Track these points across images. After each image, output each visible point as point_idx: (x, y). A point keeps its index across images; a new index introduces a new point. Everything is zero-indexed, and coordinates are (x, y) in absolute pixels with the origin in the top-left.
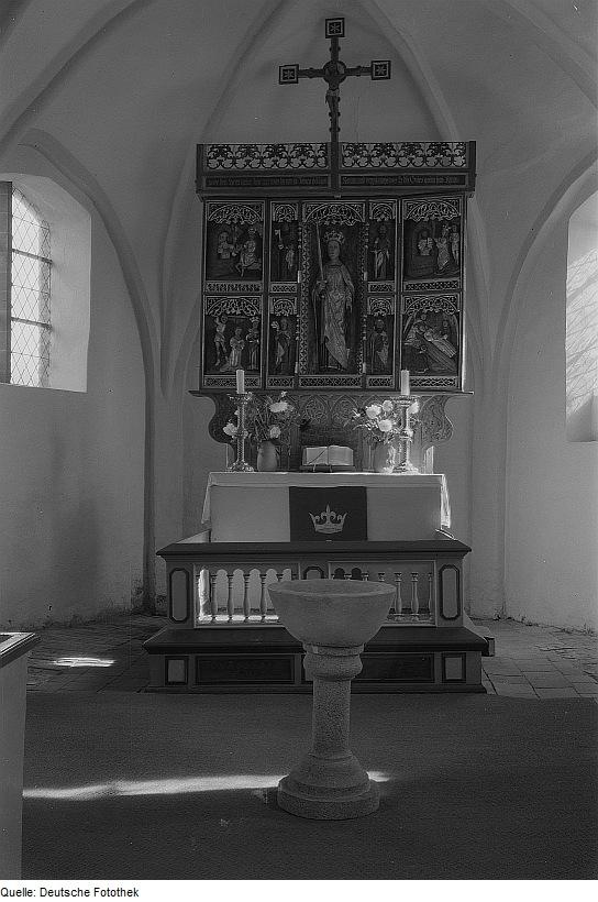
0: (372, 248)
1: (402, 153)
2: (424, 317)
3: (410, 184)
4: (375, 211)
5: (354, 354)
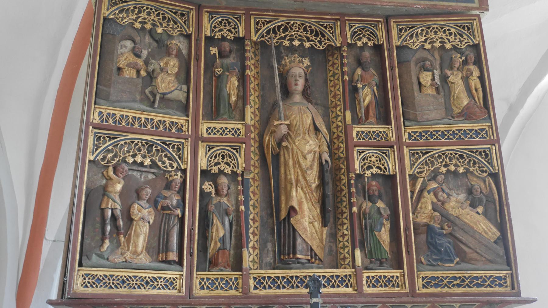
2: (441, 178)
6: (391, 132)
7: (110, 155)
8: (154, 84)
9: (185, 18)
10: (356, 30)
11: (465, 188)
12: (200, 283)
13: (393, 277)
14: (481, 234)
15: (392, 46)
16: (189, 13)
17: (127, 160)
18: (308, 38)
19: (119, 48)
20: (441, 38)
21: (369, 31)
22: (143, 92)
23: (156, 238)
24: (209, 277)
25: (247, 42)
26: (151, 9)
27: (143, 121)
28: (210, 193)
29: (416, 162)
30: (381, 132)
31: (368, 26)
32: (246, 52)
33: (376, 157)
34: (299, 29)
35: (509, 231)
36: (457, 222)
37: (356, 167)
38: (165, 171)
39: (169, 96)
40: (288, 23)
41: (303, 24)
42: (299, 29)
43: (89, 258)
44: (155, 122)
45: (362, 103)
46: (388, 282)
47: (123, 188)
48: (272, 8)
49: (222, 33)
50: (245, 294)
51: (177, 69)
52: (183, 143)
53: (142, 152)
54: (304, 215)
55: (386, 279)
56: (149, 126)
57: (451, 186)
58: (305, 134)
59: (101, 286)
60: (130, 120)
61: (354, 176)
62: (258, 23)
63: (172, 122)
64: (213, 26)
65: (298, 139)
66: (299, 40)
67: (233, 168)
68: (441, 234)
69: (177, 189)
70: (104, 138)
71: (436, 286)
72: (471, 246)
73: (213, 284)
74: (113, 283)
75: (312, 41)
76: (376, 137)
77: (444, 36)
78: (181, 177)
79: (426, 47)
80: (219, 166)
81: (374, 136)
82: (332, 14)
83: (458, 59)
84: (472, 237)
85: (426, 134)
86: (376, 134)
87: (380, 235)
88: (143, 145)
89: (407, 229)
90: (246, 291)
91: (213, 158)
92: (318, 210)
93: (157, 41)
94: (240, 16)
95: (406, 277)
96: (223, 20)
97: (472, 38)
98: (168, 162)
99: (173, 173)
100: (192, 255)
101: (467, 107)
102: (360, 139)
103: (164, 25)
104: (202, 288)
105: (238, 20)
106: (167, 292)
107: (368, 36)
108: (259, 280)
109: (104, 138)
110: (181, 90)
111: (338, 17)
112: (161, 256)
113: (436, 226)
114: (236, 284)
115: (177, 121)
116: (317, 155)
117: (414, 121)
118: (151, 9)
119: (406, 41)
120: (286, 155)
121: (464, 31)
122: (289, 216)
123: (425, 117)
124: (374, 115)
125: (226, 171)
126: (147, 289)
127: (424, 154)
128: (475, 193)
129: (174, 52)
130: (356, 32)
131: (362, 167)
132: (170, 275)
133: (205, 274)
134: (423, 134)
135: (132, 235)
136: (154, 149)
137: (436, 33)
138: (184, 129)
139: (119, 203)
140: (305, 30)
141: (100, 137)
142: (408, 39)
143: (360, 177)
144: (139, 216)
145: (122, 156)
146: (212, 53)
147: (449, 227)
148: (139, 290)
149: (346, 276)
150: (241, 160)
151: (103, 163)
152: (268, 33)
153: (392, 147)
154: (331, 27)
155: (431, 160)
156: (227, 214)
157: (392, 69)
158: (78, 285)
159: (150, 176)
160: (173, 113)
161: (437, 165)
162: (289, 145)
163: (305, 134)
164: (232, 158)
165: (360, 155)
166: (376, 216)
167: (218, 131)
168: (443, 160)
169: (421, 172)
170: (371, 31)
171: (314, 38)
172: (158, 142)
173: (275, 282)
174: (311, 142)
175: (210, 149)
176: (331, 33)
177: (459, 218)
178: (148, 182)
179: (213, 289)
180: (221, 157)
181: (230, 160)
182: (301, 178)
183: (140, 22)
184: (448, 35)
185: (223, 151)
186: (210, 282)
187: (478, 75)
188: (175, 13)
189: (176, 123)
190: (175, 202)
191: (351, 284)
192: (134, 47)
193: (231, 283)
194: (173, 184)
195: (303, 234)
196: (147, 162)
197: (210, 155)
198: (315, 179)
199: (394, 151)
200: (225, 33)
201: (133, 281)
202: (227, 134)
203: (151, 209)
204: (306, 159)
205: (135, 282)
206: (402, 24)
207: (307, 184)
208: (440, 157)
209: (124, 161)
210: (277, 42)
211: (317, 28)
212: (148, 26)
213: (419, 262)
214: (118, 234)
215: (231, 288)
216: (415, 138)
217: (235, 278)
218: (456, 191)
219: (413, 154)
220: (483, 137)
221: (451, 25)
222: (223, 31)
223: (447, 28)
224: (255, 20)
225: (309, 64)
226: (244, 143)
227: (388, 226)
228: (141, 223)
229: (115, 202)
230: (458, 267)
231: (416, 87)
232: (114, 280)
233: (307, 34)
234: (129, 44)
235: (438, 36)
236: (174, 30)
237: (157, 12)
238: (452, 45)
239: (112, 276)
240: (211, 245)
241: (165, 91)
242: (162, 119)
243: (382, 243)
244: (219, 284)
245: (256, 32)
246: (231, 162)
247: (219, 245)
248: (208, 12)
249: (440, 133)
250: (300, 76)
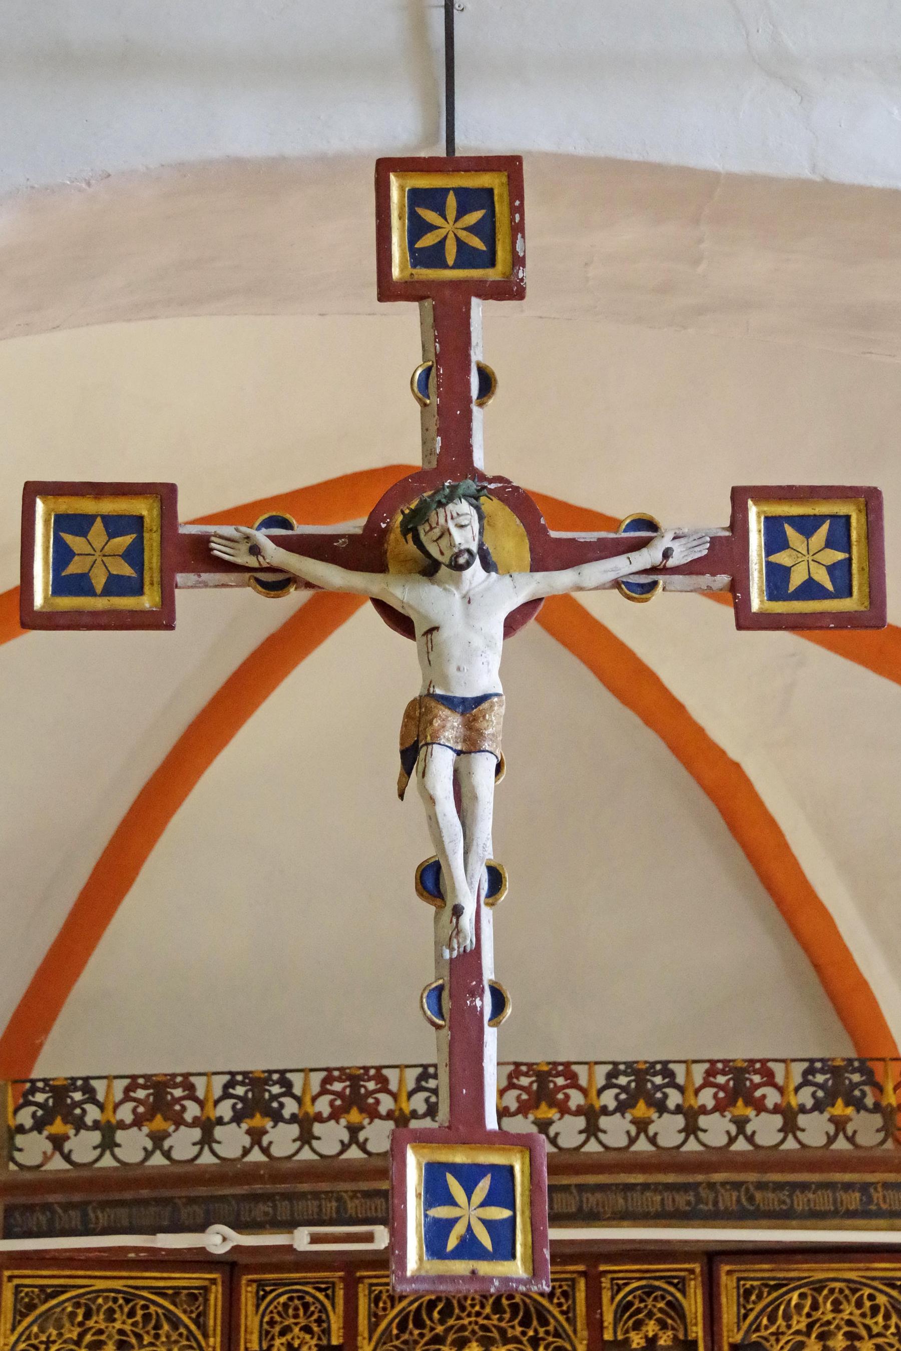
1: (707, 1098)
4: (623, 1308)
9: (197, 1308)
18: (502, 1332)
21: (663, 1298)
34: (483, 1306)
49: (289, 1337)
62: (377, 1299)
64: (266, 1319)
75: (516, 1340)
96: (291, 1299)
105: (327, 1296)
107: (659, 1315)
152: (402, 1327)
171: (519, 1329)
184: (869, 1313)
206: (752, 1275)
224: (370, 1292)
233: (501, 1319)
245: (372, 1329)
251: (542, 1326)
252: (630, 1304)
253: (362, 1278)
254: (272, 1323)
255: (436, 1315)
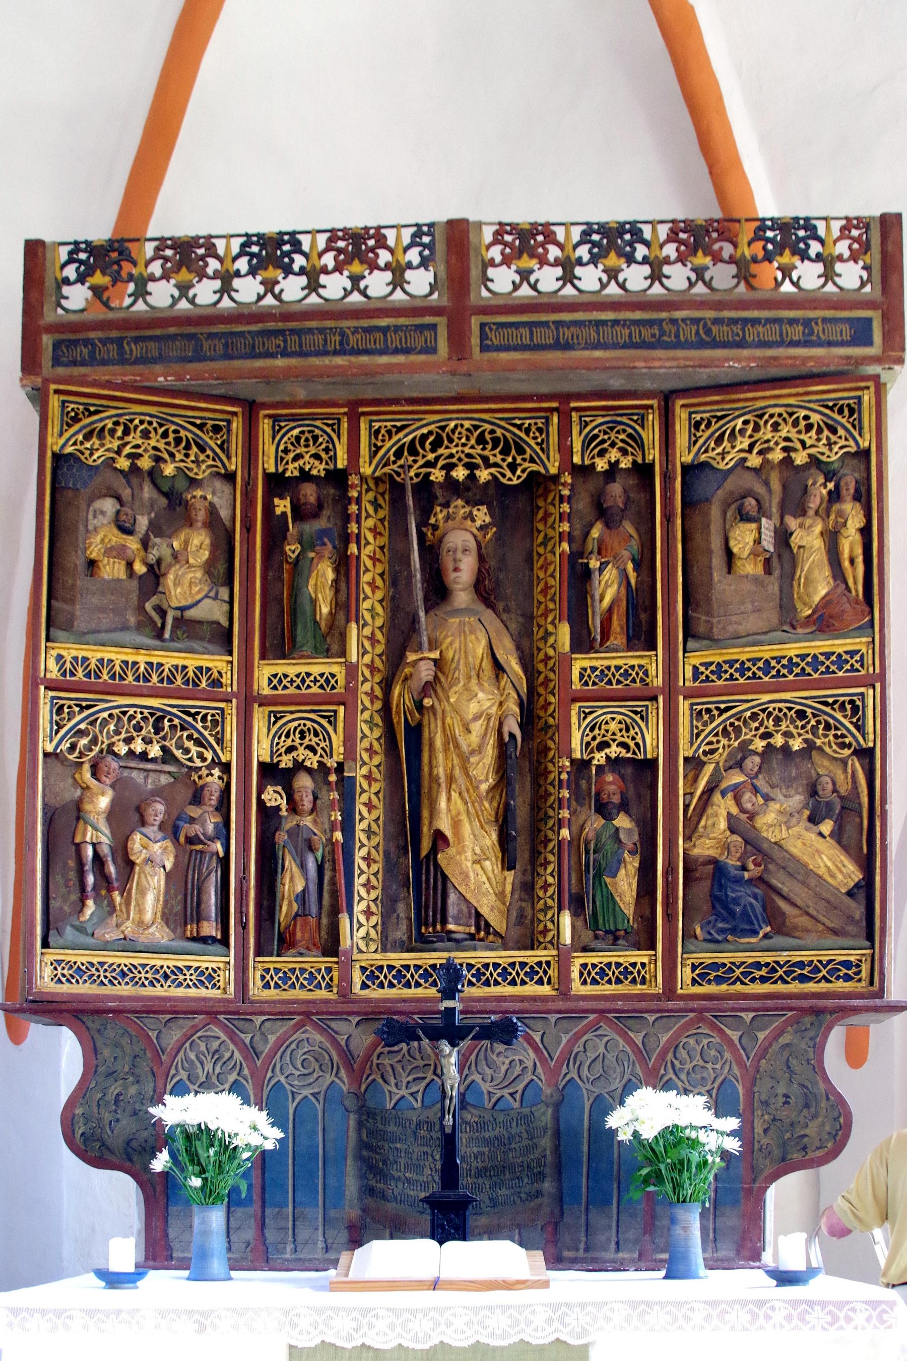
0: (579, 541)
2: (754, 762)
3: (701, 345)
5: (527, 888)
6: (654, 665)
7: (84, 741)
8: (161, 589)
10: (596, 431)
11: (805, 782)
12: (263, 978)
13: (634, 965)
14: (820, 877)
15: (674, 465)
16: (229, 422)
17: (115, 749)
18: (485, 459)
19: (90, 516)
20: (787, 439)
21: (624, 431)
22: (141, 609)
23: (180, 897)
24: (278, 966)
25: (354, 479)
26: (150, 423)
27: (142, 669)
28: (278, 808)
29: (703, 731)
30: (632, 667)
31: (624, 419)
32: (350, 503)
33: (620, 722)
34: (468, 439)
35: (878, 871)
36: (776, 853)
37: (573, 746)
38: (190, 768)
39: (191, 614)
40: (443, 428)
41: (476, 427)
42: (468, 439)
43: (60, 933)
44: (167, 670)
45: (597, 604)
46: (626, 973)
47: (114, 803)
48: (407, 394)
49: (301, 462)
50: (344, 996)
51: (207, 553)
52: (222, 710)
53: (143, 732)
54: (464, 846)
55: (621, 969)
56: (155, 678)
57: (775, 779)
58: (469, 678)
59: (85, 981)
60: (117, 668)
61: (568, 764)
62: (377, 432)
63: (200, 669)
64: (282, 447)
65: (455, 689)
66: (467, 466)
67: (321, 756)
68: (739, 881)
69: (214, 803)
70: (70, 707)
71: (719, 980)
72: (799, 902)
73: (285, 979)
74: (106, 977)
75: (496, 465)
76: (622, 679)
77: (793, 435)
78: (220, 778)
79: (748, 464)
80: (294, 754)
81: (617, 676)
82: (542, 398)
83: (820, 490)
84: (803, 883)
85: (731, 667)
86: (622, 671)
87: (615, 885)
88: (145, 719)
89: (670, 869)
90: (345, 993)
91: (283, 738)
92: (494, 836)
93: (166, 495)
94: (339, 420)
95: (659, 964)
97: (856, 434)
98: (194, 750)
99: (204, 772)
100: (244, 926)
101: (826, 601)
102: (586, 684)
103: (179, 457)
104: (267, 986)
105: (334, 430)
106: (203, 992)
107: (621, 444)
108: (372, 972)
109: (70, 707)
110: (216, 598)
111: (555, 405)
112: (191, 929)
113: (733, 862)
114: (327, 979)
115: (210, 665)
116: (494, 723)
117: (704, 639)
118: (150, 423)
119: (706, 451)
120: (432, 726)
121: (839, 418)
122: (434, 850)
123: (730, 628)
124: (622, 628)
125: (308, 764)
126: (166, 987)
127: (722, 712)
128: (820, 793)
129: (201, 516)
130: (596, 436)
131: (588, 744)
132: (208, 962)
133: (272, 961)
134: (725, 667)
135: (134, 891)
136: (167, 724)
137: (776, 427)
138: (223, 681)
139: (107, 832)
140: (481, 440)
141: (63, 705)
142: (712, 445)
143: (582, 766)
144: (143, 856)
145: (107, 742)
146: (278, 511)
147: (757, 864)
148: (152, 988)
149: (539, 964)
150: (337, 740)
151: (71, 757)
152: (399, 454)
153: (654, 699)
154: (540, 430)
155: (737, 723)
156: (311, 849)
157: (668, 521)
158: (46, 979)
159: (164, 780)
160: (201, 649)
161: (746, 734)
162: (436, 704)
163: (469, 678)
164: (321, 737)
165: (585, 718)
166: (610, 846)
167: (292, 681)
168: (761, 724)
169: (712, 752)
170: (630, 431)
171: (499, 457)
172: (174, 711)
173: (400, 975)
174: (481, 695)
175: (277, 719)
176: (537, 444)
177: (780, 847)
178: (158, 792)
179: (286, 987)
180: (298, 735)
181: (316, 739)
182: (457, 772)
183: (129, 456)
185: (302, 722)
186: (281, 975)
187: (858, 526)
188: (201, 427)
189: (208, 669)
190: (210, 828)
191: (549, 978)
192: (118, 513)
193: (319, 978)
194: (206, 792)
195: (460, 884)
196: (155, 751)
197: (276, 732)
198: (487, 774)
199: (657, 708)
200: (307, 462)
201: (140, 972)
202: (309, 687)
203: (168, 843)
204: (470, 732)
205: (143, 975)
207: (471, 783)
208: (754, 717)
209: (111, 751)
210: (417, 475)
211: (508, 434)
212: (145, 463)
213: (688, 935)
214: (110, 890)
215: (319, 986)
216: (707, 677)
217: (326, 968)
218: (784, 791)
219: (700, 713)
220: (853, 669)
221: (811, 405)
222: (302, 457)
223: (803, 413)
224: (371, 427)
225: (488, 519)
226: (343, 704)
227: (632, 863)
228: (148, 869)
229: (97, 830)
230: (767, 943)
231: (718, 561)
232: (106, 971)
233: (484, 449)
234: (109, 505)
235: (779, 434)
236: (199, 466)
237: (163, 429)
238: (810, 456)
239: (102, 964)
240: (281, 907)
241: (183, 603)
242: (181, 663)
243: (618, 899)
244: (297, 978)
246: (318, 745)
247: (295, 907)
248: (269, 416)
249: (760, 664)
250: (465, 550)
251: (519, 454)
252: (596, 437)
253: (364, 414)
254: (286, 451)
255: (428, 446)
